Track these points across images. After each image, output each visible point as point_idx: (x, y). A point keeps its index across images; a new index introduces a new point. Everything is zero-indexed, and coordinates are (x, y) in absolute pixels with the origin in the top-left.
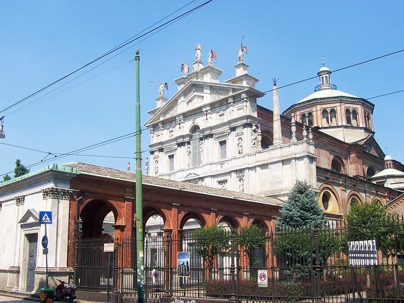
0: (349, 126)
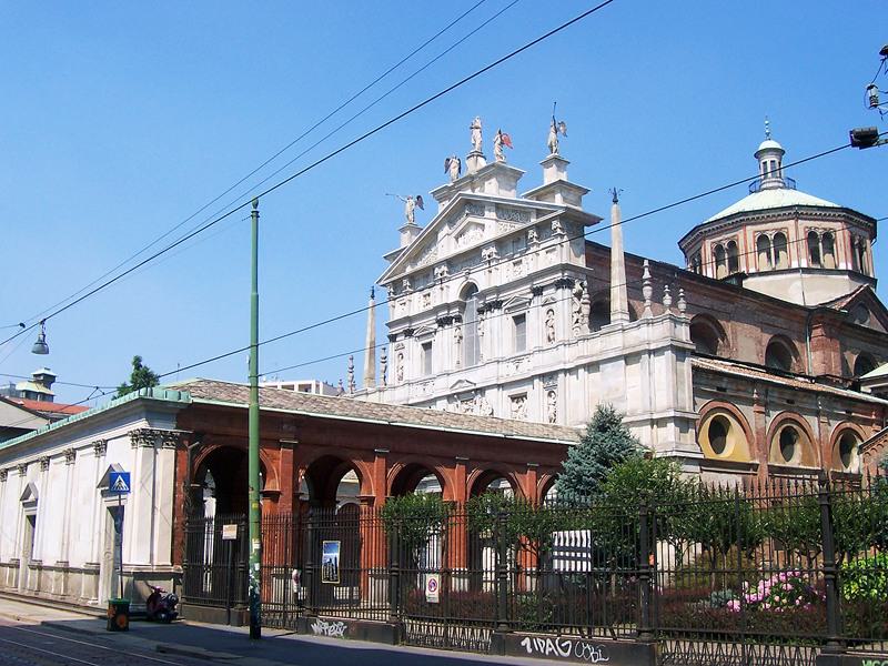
0: (817, 268)
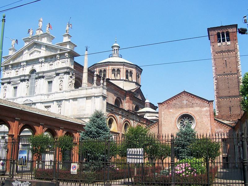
0: (127, 80)
